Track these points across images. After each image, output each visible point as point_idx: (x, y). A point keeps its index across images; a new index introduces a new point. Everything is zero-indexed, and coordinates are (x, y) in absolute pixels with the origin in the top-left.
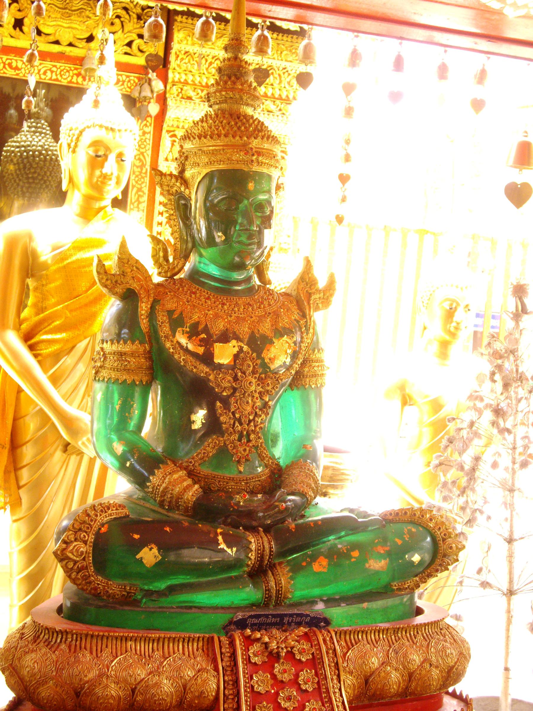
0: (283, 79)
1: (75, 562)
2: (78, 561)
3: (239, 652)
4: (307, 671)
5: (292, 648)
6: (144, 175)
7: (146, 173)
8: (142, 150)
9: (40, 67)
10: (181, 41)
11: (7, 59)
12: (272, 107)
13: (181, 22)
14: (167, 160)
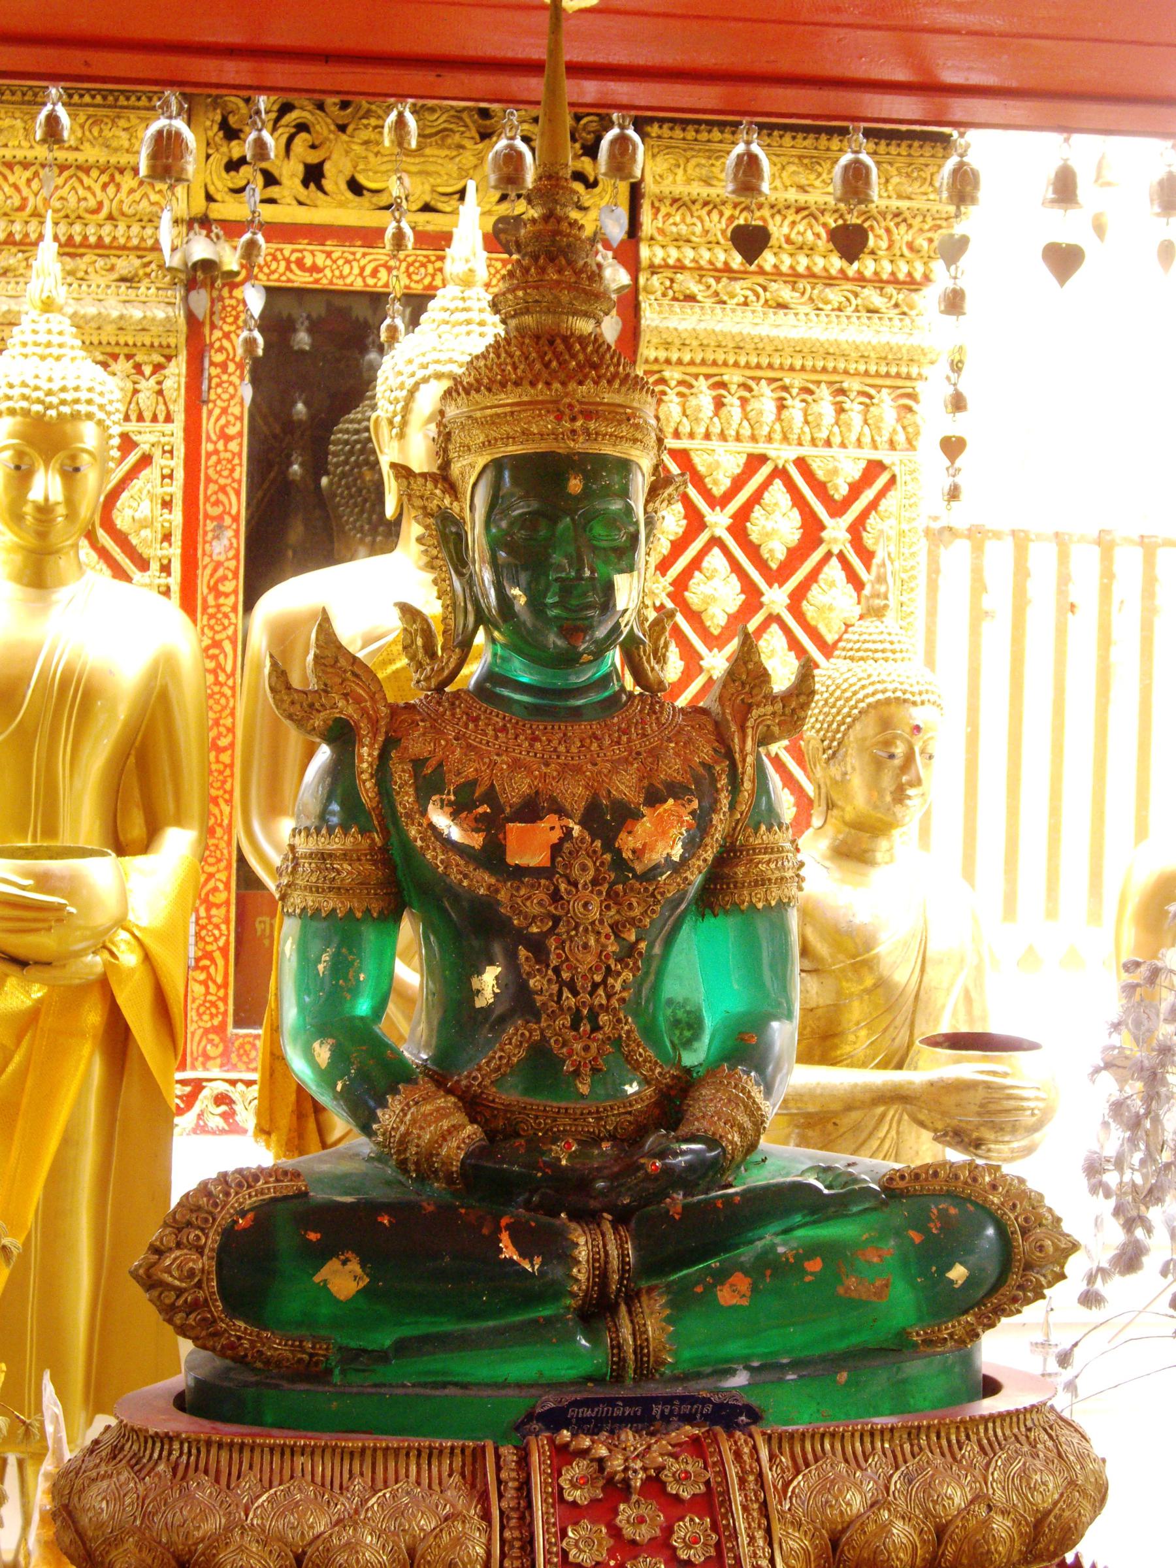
0: (896, 237)
1: (180, 1292)
2: (185, 1290)
3: (537, 1480)
4: (692, 1520)
5: (660, 1469)
9: (363, 262)
11: (293, 251)
12: (877, 300)
13: (659, 137)
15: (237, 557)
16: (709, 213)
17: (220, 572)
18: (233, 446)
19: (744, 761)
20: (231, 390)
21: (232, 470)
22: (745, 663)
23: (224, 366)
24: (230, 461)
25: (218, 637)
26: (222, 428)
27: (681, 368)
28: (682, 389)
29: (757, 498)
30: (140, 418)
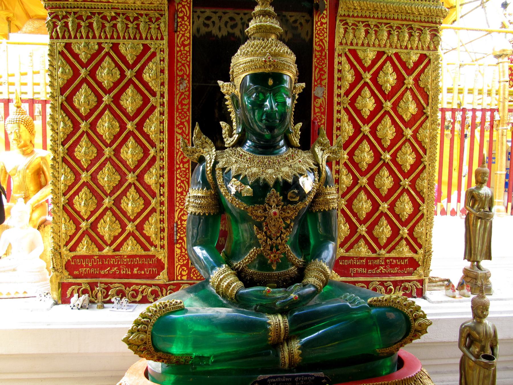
6: (323, 58)
7: (325, 56)
8: (321, 38)
14: (341, 44)
15: (189, 90)
17: (183, 96)
18: (187, 48)
20: (186, 27)
21: (187, 58)
23: (183, 18)
24: (186, 54)
25: (183, 121)
26: (183, 41)
29: (381, 68)
30: (152, 38)
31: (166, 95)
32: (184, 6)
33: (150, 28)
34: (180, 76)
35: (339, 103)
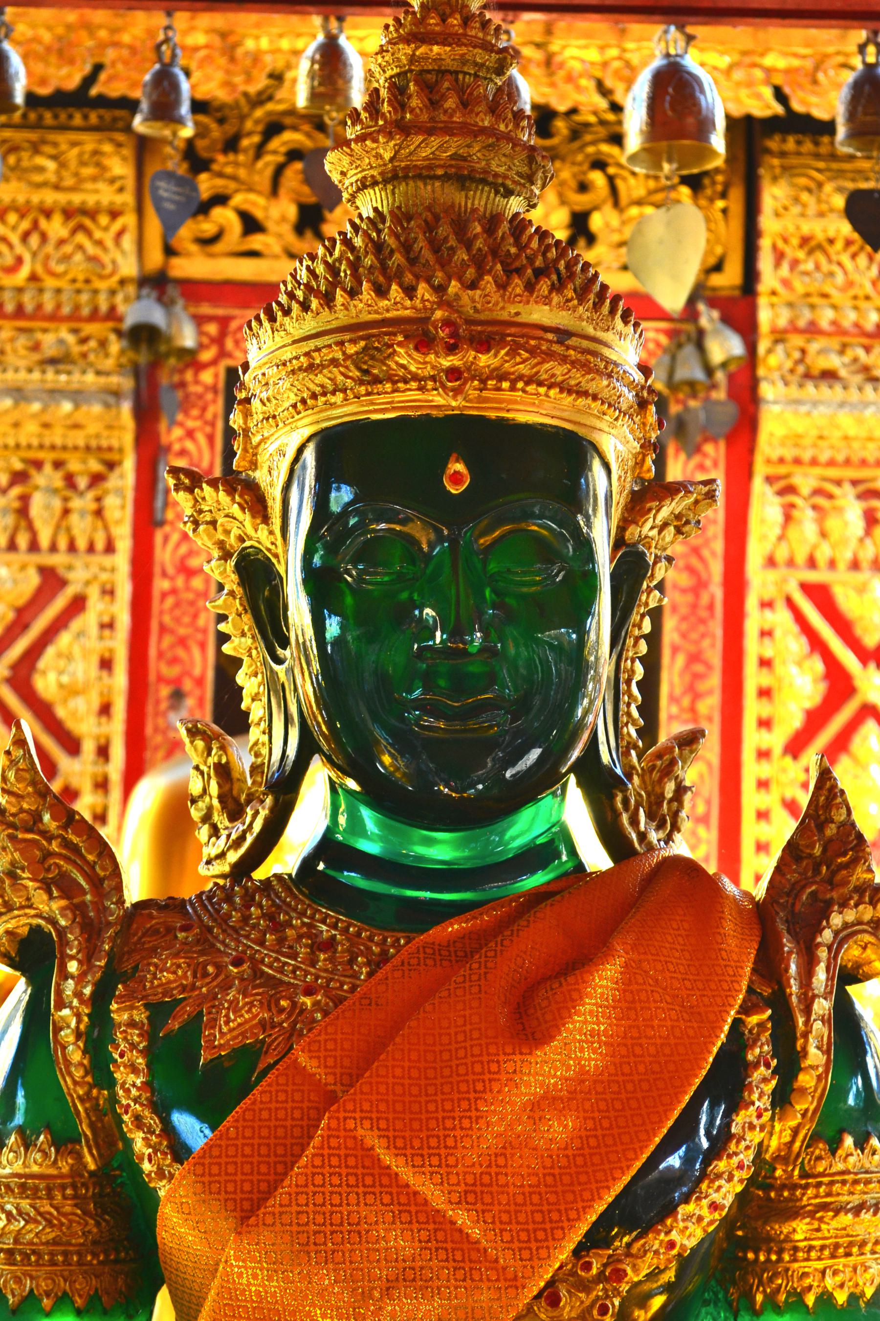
6: (703, 614)
7: (711, 607)
10: (786, 208)
14: (771, 562)
16: (854, 256)
19: (808, 1011)
22: (821, 827)
24: (192, 603)
26: (183, 559)
27: (817, 471)
28: (821, 501)
31: (118, 752)
32: (190, 434)
33: (66, 512)
34: (168, 682)
35: (763, 784)
